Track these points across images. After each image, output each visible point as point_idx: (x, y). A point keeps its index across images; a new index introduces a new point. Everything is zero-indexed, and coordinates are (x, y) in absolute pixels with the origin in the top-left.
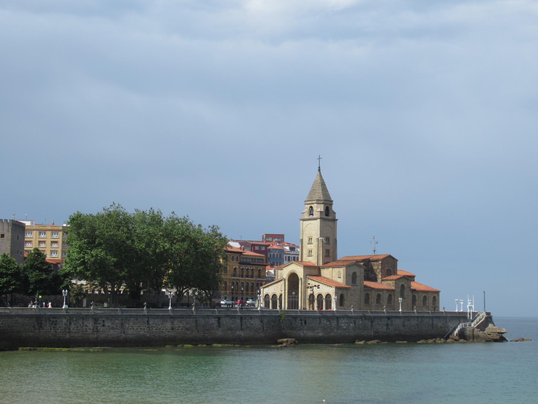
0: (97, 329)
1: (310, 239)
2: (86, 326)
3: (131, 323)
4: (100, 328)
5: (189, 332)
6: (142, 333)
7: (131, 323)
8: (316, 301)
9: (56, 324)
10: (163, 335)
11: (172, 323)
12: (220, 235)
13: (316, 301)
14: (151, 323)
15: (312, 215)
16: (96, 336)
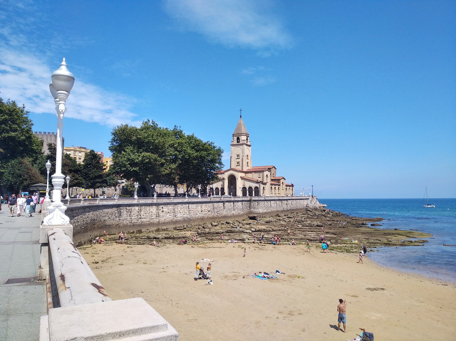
0: (159, 214)
1: (238, 156)
2: (152, 212)
3: (179, 209)
4: (161, 214)
5: (210, 213)
6: (185, 215)
7: (179, 209)
8: (247, 192)
9: (131, 212)
10: (197, 216)
11: (201, 207)
12: (214, 147)
13: (247, 192)
14: (190, 207)
15: (239, 142)
16: (158, 220)
